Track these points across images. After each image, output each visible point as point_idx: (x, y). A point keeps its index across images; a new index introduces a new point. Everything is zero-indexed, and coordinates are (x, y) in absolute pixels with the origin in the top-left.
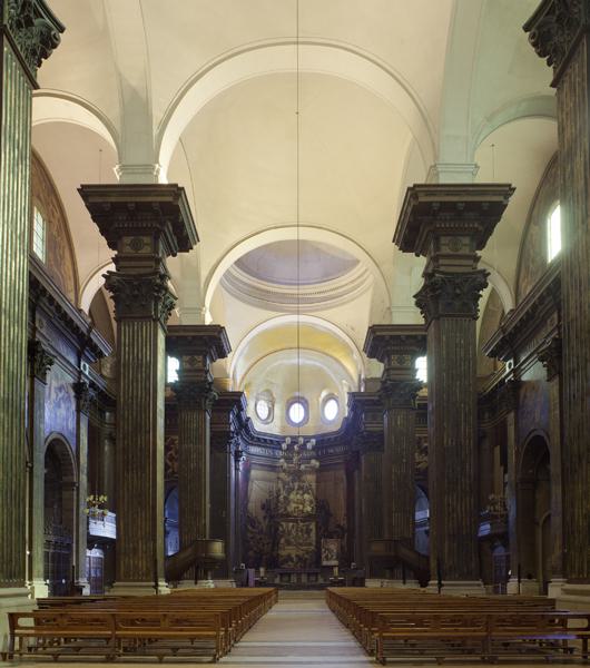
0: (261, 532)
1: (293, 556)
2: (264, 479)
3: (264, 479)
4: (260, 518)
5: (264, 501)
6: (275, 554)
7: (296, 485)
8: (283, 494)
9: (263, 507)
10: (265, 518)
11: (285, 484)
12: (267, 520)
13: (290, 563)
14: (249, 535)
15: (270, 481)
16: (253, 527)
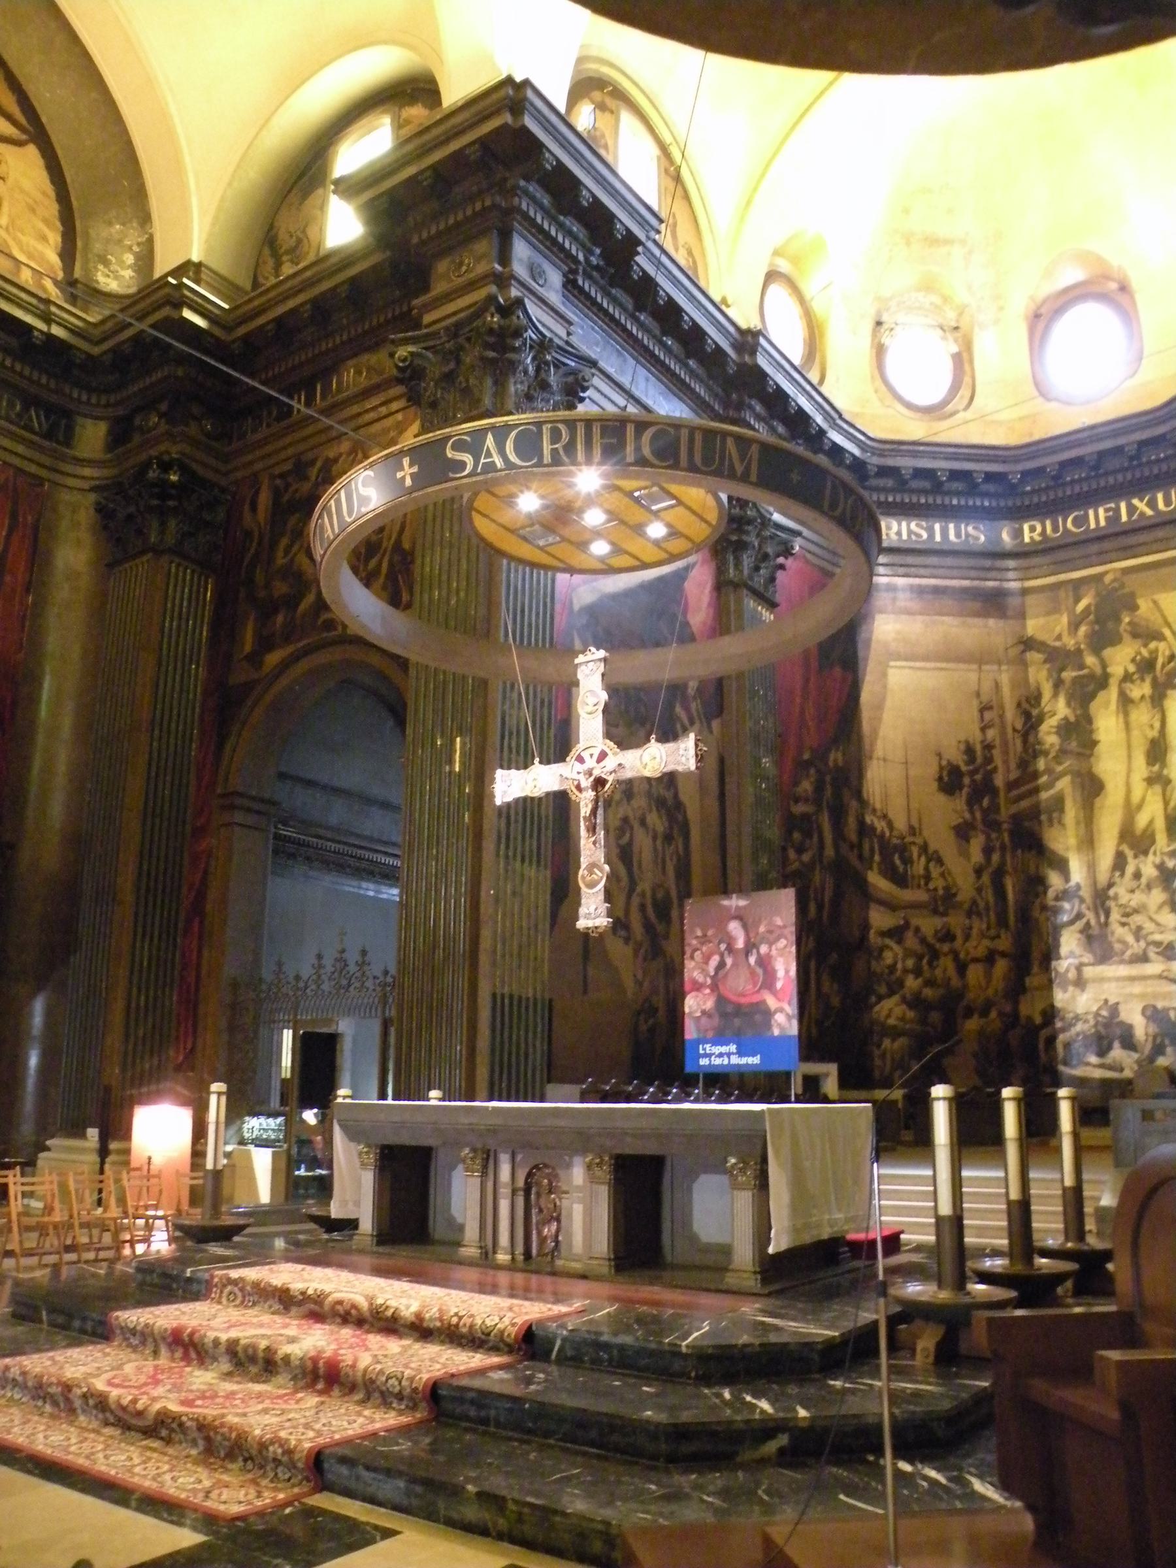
0: (944, 902)
1: (1135, 1018)
2: (949, 655)
3: (949, 655)
4: (940, 838)
5: (955, 755)
6: (1030, 1009)
7: (1121, 658)
8: (1059, 709)
9: (950, 780)
10: (963, 832)
11: (1058, 658)
12: (976, 845)
13: (1117, 1053)
14: (879, 919)
15: (979, 658)
16: (901, 880)
